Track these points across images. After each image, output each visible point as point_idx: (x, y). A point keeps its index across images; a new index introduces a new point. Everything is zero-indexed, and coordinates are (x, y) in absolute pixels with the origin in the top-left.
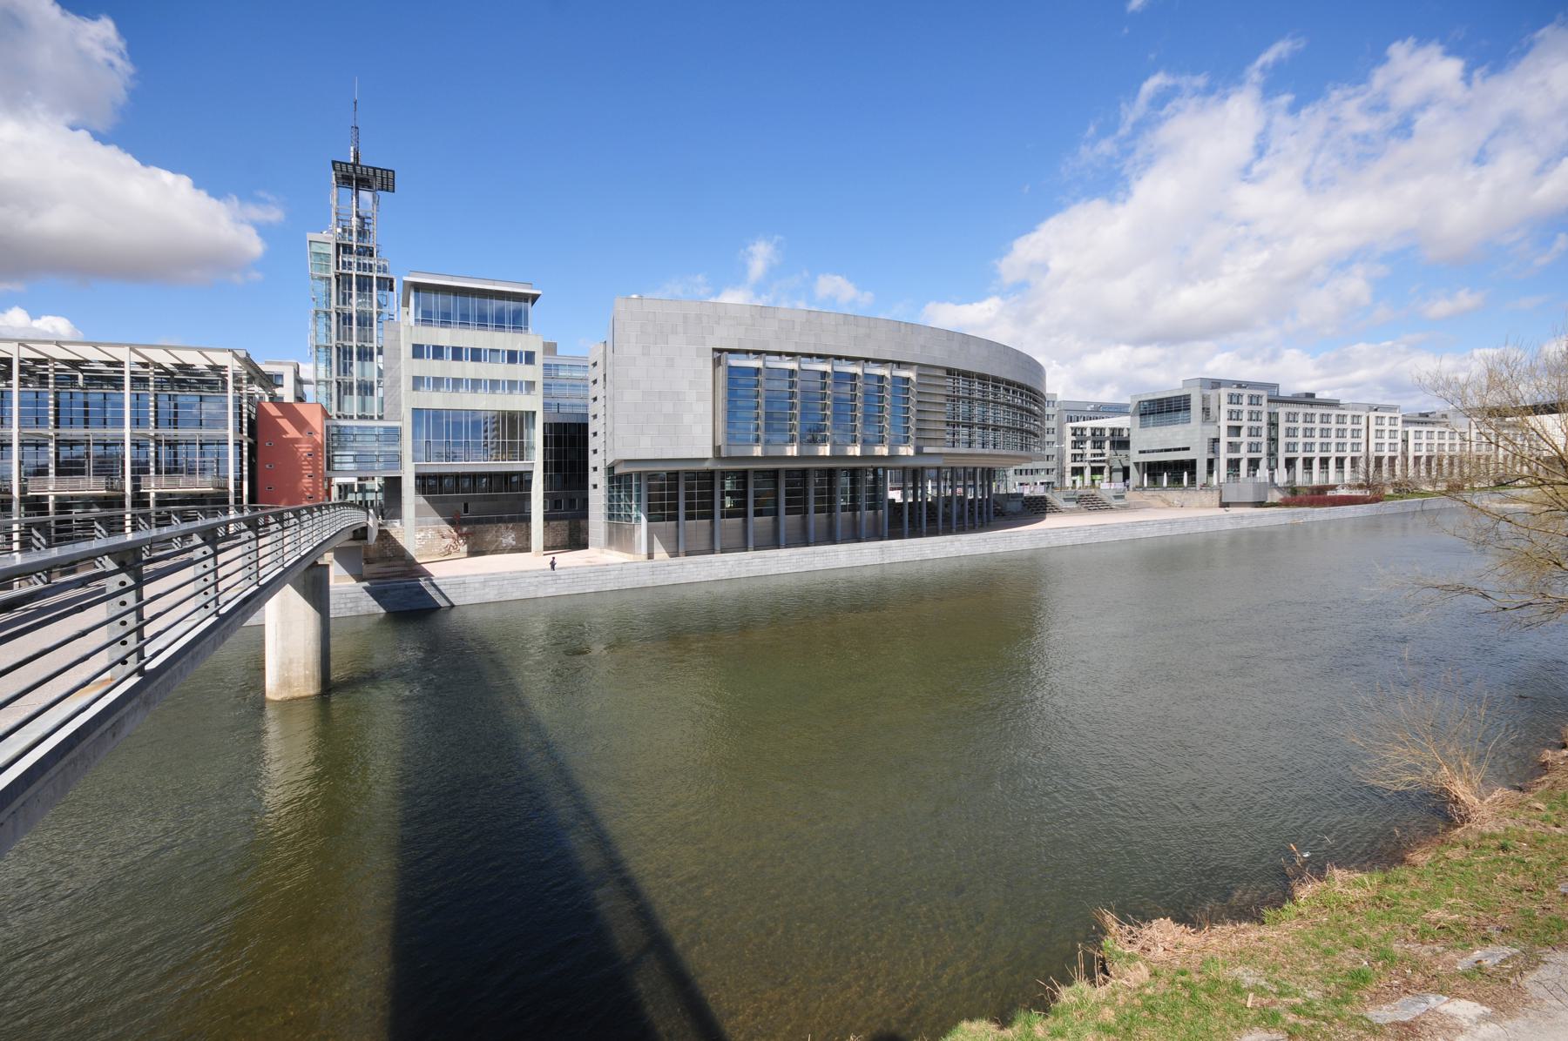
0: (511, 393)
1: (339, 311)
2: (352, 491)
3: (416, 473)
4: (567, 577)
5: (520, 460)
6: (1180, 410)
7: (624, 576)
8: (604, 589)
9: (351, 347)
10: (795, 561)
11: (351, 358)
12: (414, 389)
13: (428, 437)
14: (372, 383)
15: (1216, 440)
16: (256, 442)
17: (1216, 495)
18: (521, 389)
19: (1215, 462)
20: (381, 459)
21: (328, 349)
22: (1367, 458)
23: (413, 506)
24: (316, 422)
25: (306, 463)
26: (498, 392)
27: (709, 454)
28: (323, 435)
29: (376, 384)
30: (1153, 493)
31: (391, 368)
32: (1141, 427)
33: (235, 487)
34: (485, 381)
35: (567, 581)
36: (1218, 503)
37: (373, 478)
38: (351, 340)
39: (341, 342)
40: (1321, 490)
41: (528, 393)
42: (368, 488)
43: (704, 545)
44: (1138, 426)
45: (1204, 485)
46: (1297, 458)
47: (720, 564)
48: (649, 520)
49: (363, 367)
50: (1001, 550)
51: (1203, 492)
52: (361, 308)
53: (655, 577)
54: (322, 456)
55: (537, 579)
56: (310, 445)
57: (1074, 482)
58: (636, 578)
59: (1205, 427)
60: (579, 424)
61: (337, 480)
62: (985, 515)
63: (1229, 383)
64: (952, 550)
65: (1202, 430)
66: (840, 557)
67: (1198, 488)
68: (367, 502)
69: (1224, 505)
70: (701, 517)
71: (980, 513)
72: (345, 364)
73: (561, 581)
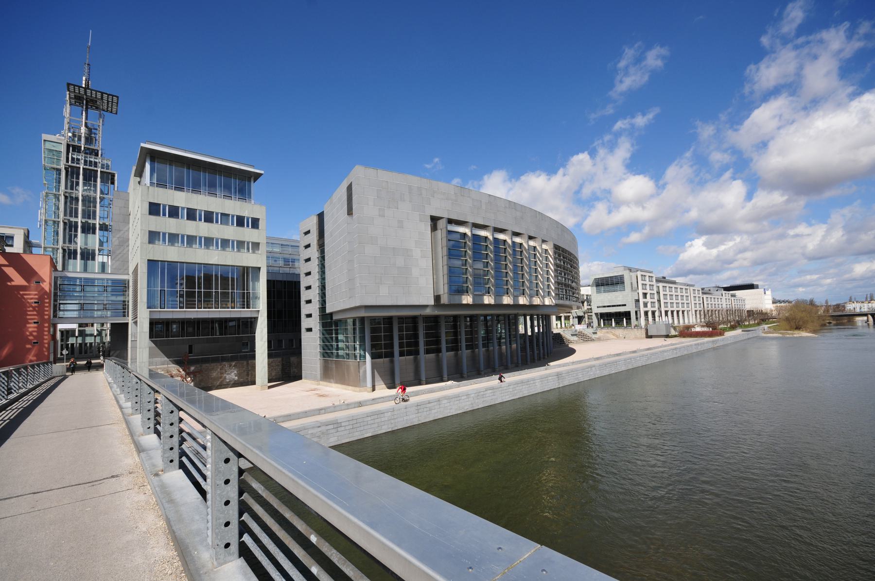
0: (239, 251)
1: (67, 195)
2: (73, 335)
3: (151, 320)
4: (347, 423)
5: (248, 308)
6: (619, 283)
7: (395, 417)
8: (379, 432)
9: (76, 223)
10: (511, 390)
11: (76, 231)
12: (150, 243)
13: (162, 286)
14: (94, 251)
15: (638, 301)
18: (248, 249)
19: (638, 312)
21: (56, 223)
22: (704, 311)
23: (148, 349)
24: (44, 271)
25: (31, 309)
26: (228, 249)
27: (432, 302)
28: (50, 284)
29: (97, 252)
30: (607, 330)
31: (120, 231)
35: (347, 428)
36: (645, 336)
37: (92, 325)
38: (76, 216)
40: (688, 327)
41: (254, 252)
43: (411, 376)
45: (636, 326)
47: (465, 397)
48: (373, 358)
49: (86, 238)
50: (613, 372)
52: (86, 193)
53: (419, 415)
54: (49, 303)
55: (320, 429)
57: (557, 324)
58: (405, 418)
59: (633, 293)
60: (285, 281)
61: (60, 326)
62: (541, 347)
64: (592, 373)
65: (632, 294)
67: (633, 327)
69: (649, 336)
70: (409, 353)
71: (538, 345)
72: (70, 236)
73: (343, 428)
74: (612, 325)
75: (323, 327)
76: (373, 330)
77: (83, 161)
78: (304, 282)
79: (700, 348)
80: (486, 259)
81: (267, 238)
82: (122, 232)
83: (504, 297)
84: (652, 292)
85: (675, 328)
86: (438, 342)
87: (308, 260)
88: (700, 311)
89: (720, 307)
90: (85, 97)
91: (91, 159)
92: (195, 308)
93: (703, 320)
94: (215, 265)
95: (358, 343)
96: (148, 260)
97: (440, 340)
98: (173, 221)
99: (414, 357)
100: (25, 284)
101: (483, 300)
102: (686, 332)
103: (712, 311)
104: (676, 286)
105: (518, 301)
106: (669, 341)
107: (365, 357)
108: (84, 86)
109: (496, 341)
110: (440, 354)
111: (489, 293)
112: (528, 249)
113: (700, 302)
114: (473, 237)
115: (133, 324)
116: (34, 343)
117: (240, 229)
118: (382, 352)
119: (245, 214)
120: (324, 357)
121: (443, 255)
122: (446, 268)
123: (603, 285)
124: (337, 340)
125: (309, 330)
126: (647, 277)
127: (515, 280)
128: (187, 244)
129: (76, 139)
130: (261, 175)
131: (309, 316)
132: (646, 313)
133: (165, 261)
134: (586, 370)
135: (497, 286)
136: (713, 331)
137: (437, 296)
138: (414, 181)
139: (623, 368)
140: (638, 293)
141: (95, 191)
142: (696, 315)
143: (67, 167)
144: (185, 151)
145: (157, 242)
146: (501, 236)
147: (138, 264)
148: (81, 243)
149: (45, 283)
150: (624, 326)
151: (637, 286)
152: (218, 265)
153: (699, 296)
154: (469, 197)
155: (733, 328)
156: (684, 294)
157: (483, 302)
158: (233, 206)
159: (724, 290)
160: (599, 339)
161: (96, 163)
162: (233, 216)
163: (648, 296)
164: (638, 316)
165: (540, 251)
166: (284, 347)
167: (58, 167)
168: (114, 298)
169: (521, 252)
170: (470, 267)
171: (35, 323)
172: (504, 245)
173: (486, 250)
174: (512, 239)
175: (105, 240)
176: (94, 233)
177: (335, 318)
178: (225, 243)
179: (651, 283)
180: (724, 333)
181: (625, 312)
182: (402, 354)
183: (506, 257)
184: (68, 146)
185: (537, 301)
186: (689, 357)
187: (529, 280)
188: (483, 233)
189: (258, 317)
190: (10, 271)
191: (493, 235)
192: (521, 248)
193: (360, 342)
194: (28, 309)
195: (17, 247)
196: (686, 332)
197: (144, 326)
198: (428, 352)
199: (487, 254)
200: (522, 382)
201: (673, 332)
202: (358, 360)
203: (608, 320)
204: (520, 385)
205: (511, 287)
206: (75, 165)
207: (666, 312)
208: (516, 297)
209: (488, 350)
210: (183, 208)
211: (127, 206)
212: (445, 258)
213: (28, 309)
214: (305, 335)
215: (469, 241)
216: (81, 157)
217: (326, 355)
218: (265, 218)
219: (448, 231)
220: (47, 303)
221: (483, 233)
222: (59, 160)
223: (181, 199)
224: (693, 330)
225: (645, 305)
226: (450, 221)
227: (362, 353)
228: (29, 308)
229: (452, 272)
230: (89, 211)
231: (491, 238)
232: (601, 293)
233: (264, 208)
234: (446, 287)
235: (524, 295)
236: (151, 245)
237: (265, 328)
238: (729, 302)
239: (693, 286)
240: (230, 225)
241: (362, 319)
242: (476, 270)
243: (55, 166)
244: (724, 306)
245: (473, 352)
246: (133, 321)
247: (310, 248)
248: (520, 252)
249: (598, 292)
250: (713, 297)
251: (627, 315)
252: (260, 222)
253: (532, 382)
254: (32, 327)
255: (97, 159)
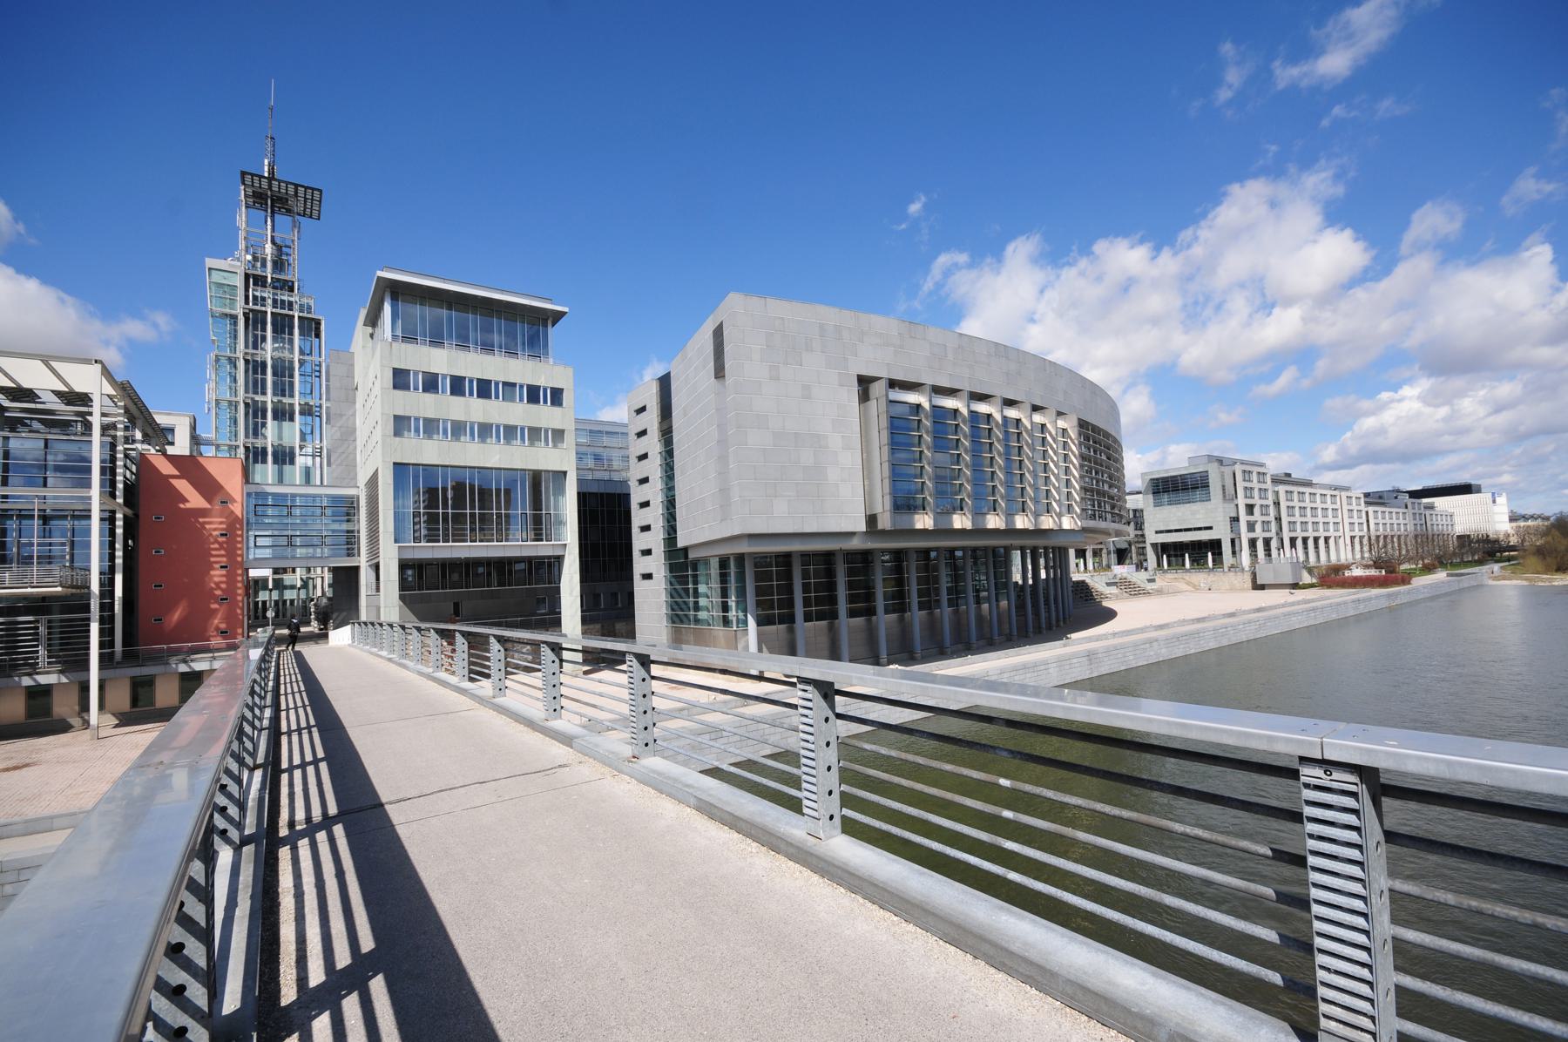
0: (532, 444)
1: (249, 358)
3: (400, 560)
6: (1198, 488)
11: (264, 416)
14: (292, 449)
15: (1235, 520)
16: (136, 515)
17: (1248, 578)
19: (1237, 542)
20: (328, 540)
22: (1370, 538)
25: (216, 546)
26: (514, 442)
27: (862, 527)
29: (297, 451)
30: (1176, 576)
31: (341, 415)
32: (1155, 506)
33: (102, 585)
34: (498, 427)
36: (1250, 585)
38: (264, 393)
39: (251, 395)
40: (1338, 569)
41: (555, 446)
42: (287, 583)
44: (1153, 504)
45: (1232, 566)
46: (1297, 537)
48: (759, 624)
50: (1193, 651)
51: (1232, 574)
52: (279, 354)
56: (224, 520)
60: (602, 494)
62: (1053, 606)
63: (1243, 463)
64: (1152, 653)
65: (1224, 508)
66: (1051, 671)
67: (1226, 569)
68: (285, 601)
69: (1258, 587)
71: (1047, 602)
74: (1184, 565)
75: (671, 572)
76: (759, 577)
77: (270, 301)
78: (636, 497)
79: (1362, 608)
80: (957, 448)
81: (577, 421)
82: (344, 418)
83: (988, 517)
84: (1264, 502)
85: (1310, 571)
86: (869, 597)
87: (644, 457)
88: (1361, 538)
89: (1402, 530)
90: (269, 193)
91: (283, 298)
92: (465, 541)
93: (1367, 555)
94: (496, 469)
95: (733, 598)
96: (394, 464)
97: (874, 592)
98: (429, 397)
99: (929, 614)
100: (208, 506)
101: (951, 522)
102: (1332, 577)
103: (1385, 537)
104: (1313, 491)
105: (1013, 522)
106: (1300, 595)
107: (745, 622)
108: (266, 175)
109: (971, 595)
110: (874, 618)
111: (962, 510)
112: (1032, 430)
113: (1360, 521)
114: (934, 411)
115: (368, 568)
116: (221, 599)
117: (533, 407)
118: (815, 606)
119: (541, 382)
120: (673, 622)
121: (882, 444)
122: (886, 466)
123: (1166, 491)
124: (696, 594)
125: (648, 576)
126: (1254, 474)
127: (1009, 486)
128: (452, 435)
129: (259, 264)
130: (563, 314)
131: (647, 552)
132: (1253, 543)
133: (419, 465)
134: (1142, 647)
135: (977, 497)
136: (1389, 575)
137: (870, 516)
138: (830, 315)
139: (1213, 645)
140: (1237, 505)
141: (291, 351)
142: (1353, 546)
143: (247, 311)
144: (444, 280)
145: (406, 433)
146: (982, 408)
147: (377, 470)
148: (273, 435)
149: (235, 504)
150: (1209, 568)
151: (1233, 492)
152: (500, 469)
153: (1359, 508)
154: (925, 339)
155: (1428, 569)
156: (1329, 505)
157: (985, 525)
158: (521, 370)
159: (1410, 497)
160: (1160, 592)
161: (291, 304)
162: (521, 387)
163: (1257, 510)
164: (1237, 548)
165: (1054, 433)
166: (602, 607)
167: (233, 312)
168: (336, 526)
169: (1019, 434)
170: (929, 464)
171: (222, 567)
172: (988, 423)
173: (956, 433)
174: (1002, 411)
175: (309, 431)
176: (292, 419)
177: (692, 555)
178: (510, 432)
179: (1263, 486)
180: (1410, 579)
181: (1210, 540)
182: (808, 618)
183: (991, 444)
184: (247, 276)
185: (1047, 523)
186: (1343, 623)
187: (1034, 485)
188: (949, 403)
189: (564, 556)
190: (183, 486)
191: (969, 406)
192: (1017, 428)
193: (737, 597)
194: (212, 546)
195: (181, 446)
196: (1332, 577)
197: (390, 573)
198: (853, 614)
199: (958, 440)
200: (1025, 667)
201: (1307, 578)
202: (735, 628)
203: (1176, 556)
204: (1021, 672)
205: (1002, 498)
206: (258, 307)
207: (1293, 541)
208: (1010, 515)
209: (956, 612)
210: (444, 377)
211: (351, 375)
212: (886, 449)
213: (212, 546)
214: (640, 586)
215: (927, 418)
216: (267, 294)
217: (676, 619)
218: (572, 388)
219: (891, 401)
220: (239, 536)
221: (949, 403)
222: (233, 301)
223: (443, 360)
224: (1346, 575)
225: (1251, 527)
226: (893, 384)
227: (741, 615)
228: (213, 544)
229: (896, 474)
230: (283, 384)
231: (964, 411)
232: (1164, 505)
233: (570, 371)
234: (888, 499)
235: (1024, 511)
236: (398, 439)
237: (576, 573)
238: (1421, 520)
239: (1347, 489)
240: (518, 401)
241: (740, 558)
242: (938, 469)
243: (228, 311)
244: (1410, 528)
245: (931, 614)
246: (368, 564)
247: (645, 436)
248: (1016, 435)
249: (1156, 505)
250: (1387, 510)
251: (1215, 546)
252: (565, 394)
253: (1042, 667)
254: (217, 575)
255: (292, 296)
